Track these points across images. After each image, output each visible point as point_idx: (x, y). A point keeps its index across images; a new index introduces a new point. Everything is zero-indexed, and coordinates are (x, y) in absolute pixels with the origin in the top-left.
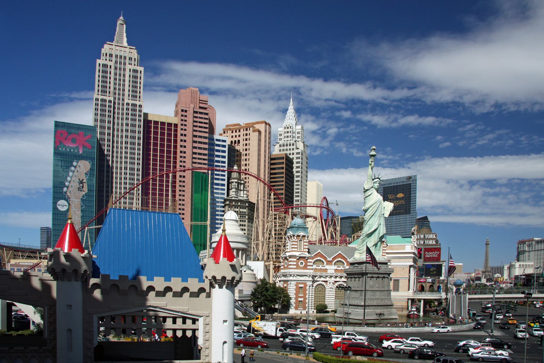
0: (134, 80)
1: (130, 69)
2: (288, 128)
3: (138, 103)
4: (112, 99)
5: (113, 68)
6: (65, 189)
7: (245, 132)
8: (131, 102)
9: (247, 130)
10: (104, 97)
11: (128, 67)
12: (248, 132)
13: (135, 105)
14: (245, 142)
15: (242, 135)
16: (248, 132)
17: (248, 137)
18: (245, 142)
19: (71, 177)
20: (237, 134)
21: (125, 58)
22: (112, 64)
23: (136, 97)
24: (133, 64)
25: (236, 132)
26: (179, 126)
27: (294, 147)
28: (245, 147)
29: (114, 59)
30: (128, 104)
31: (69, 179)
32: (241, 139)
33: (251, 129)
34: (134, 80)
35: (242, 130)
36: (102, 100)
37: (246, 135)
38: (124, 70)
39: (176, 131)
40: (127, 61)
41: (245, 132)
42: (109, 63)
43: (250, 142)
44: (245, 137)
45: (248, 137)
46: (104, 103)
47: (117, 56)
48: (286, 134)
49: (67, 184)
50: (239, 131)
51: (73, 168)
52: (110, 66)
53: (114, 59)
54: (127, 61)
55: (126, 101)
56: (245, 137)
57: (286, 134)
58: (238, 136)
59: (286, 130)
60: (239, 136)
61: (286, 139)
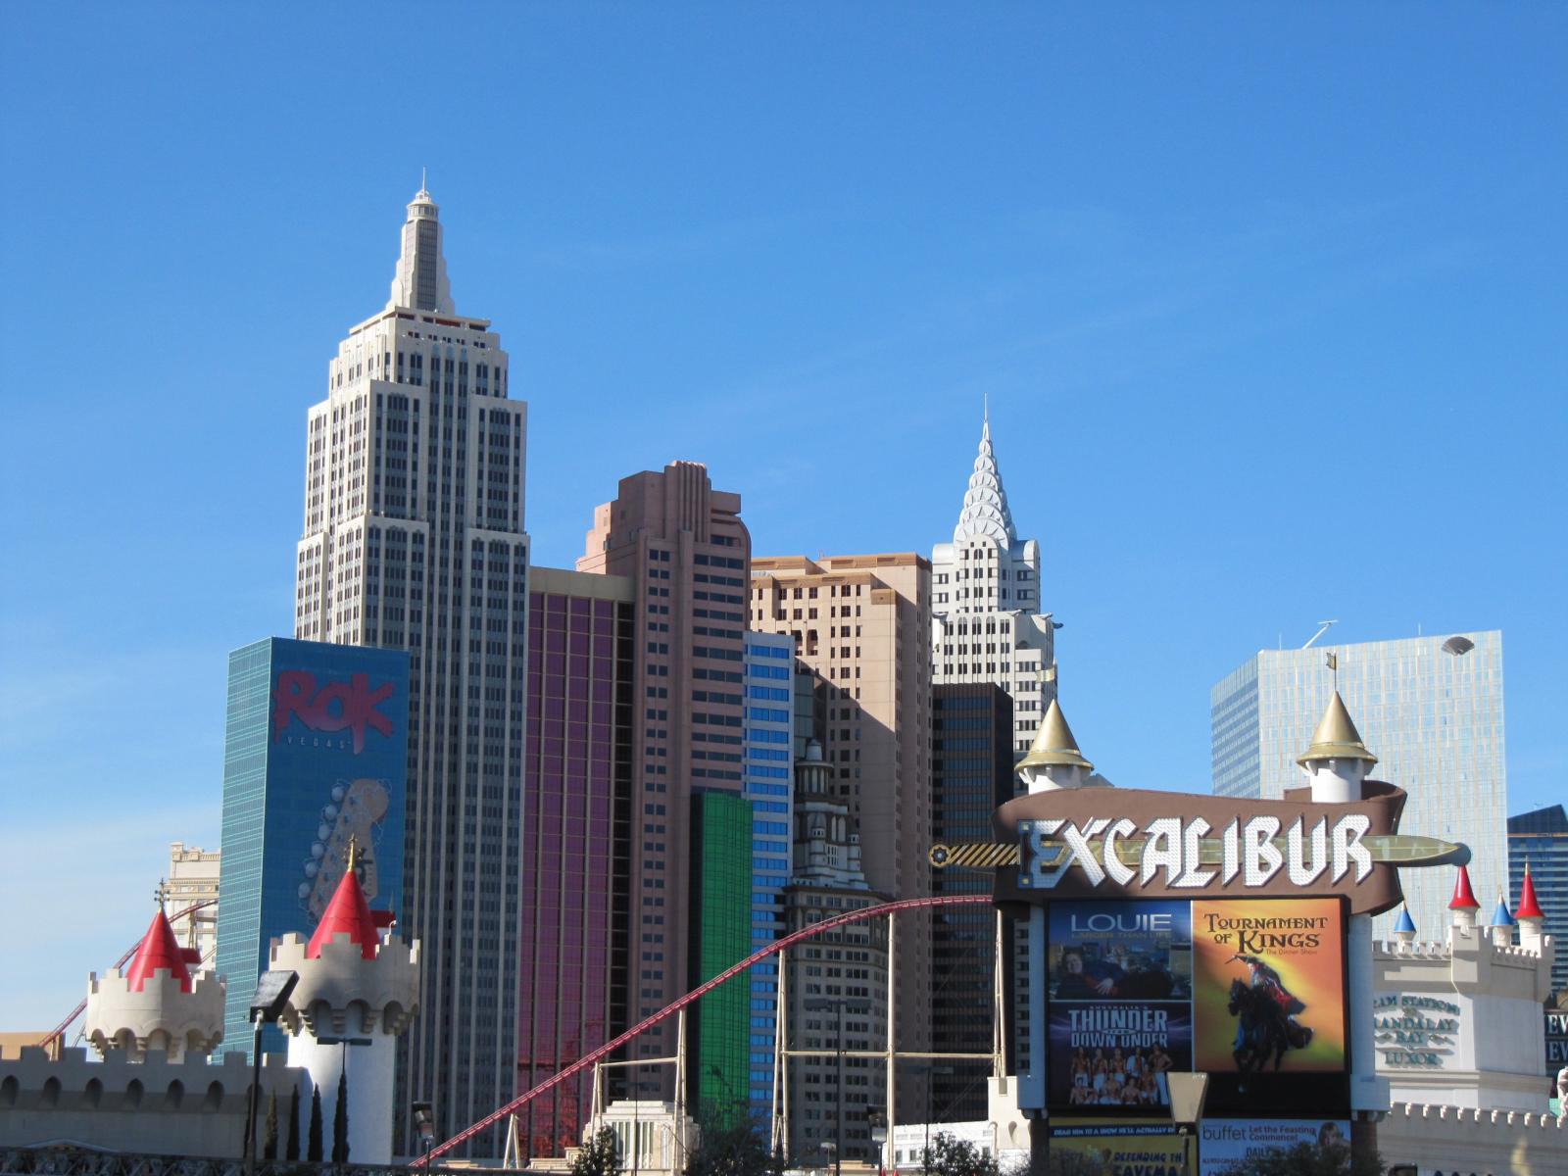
0: (497, 450)
1: (482, 412)
2: (978, 555)
3: (511, 539)
4: (424, 528)
5: (424, 408)
6: (304, 888)
7: (839, 601)
8: (488, 536)
9: (846, 592)
10: (398, 523)
11: (477, 402)
12: (851, 601)
13: (499, 548)
14: (840, 642)
15: (824, 612)
16: (851, 601)
17: (851, 622)
18: (840, 642)
19: (325, 844)
20: (805, 604)
21: (464, 367)
22: (421, 393)
23: (502, 514)
24: (491, 390)
25: (798, 595)
26: (641, 610)
27: (1011, 638)
28: (839, 663)
29: (426, 375)
30: (478, 545)
31: (316, 849)
32: (822, 626)
33: (866, 589)
34: (497, 450)
35: (824, 591)
36: (395, 535)
37: (846, 611)
38: (463, 413)
39: (627, 629)
40: (472, 380)
41: (839, 601)
42: (412, 392)
43: (860, 642)
44: (839, 622)
45: (851, 622)
46: (397, 546)
47: (435, 363)
48: (971, 583)
49: (310, 868)
50: (813, 594)
51: (330, 810)
52: (416, 402)
53: (426, 375)
54: (472, 380)
55: (471, 534)
56: (839, 622)
57: (971, 583)
58: (805, 614)
59: (971, 564)
60: (813, 614)
61: (971, 602)
